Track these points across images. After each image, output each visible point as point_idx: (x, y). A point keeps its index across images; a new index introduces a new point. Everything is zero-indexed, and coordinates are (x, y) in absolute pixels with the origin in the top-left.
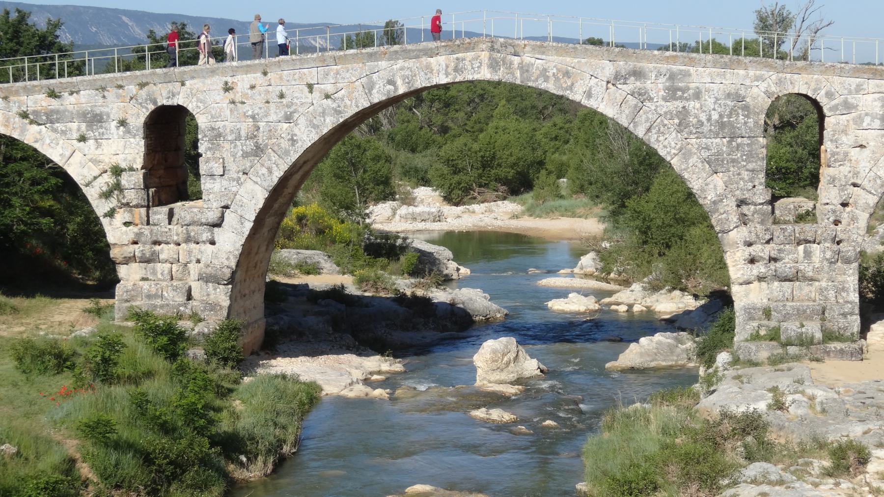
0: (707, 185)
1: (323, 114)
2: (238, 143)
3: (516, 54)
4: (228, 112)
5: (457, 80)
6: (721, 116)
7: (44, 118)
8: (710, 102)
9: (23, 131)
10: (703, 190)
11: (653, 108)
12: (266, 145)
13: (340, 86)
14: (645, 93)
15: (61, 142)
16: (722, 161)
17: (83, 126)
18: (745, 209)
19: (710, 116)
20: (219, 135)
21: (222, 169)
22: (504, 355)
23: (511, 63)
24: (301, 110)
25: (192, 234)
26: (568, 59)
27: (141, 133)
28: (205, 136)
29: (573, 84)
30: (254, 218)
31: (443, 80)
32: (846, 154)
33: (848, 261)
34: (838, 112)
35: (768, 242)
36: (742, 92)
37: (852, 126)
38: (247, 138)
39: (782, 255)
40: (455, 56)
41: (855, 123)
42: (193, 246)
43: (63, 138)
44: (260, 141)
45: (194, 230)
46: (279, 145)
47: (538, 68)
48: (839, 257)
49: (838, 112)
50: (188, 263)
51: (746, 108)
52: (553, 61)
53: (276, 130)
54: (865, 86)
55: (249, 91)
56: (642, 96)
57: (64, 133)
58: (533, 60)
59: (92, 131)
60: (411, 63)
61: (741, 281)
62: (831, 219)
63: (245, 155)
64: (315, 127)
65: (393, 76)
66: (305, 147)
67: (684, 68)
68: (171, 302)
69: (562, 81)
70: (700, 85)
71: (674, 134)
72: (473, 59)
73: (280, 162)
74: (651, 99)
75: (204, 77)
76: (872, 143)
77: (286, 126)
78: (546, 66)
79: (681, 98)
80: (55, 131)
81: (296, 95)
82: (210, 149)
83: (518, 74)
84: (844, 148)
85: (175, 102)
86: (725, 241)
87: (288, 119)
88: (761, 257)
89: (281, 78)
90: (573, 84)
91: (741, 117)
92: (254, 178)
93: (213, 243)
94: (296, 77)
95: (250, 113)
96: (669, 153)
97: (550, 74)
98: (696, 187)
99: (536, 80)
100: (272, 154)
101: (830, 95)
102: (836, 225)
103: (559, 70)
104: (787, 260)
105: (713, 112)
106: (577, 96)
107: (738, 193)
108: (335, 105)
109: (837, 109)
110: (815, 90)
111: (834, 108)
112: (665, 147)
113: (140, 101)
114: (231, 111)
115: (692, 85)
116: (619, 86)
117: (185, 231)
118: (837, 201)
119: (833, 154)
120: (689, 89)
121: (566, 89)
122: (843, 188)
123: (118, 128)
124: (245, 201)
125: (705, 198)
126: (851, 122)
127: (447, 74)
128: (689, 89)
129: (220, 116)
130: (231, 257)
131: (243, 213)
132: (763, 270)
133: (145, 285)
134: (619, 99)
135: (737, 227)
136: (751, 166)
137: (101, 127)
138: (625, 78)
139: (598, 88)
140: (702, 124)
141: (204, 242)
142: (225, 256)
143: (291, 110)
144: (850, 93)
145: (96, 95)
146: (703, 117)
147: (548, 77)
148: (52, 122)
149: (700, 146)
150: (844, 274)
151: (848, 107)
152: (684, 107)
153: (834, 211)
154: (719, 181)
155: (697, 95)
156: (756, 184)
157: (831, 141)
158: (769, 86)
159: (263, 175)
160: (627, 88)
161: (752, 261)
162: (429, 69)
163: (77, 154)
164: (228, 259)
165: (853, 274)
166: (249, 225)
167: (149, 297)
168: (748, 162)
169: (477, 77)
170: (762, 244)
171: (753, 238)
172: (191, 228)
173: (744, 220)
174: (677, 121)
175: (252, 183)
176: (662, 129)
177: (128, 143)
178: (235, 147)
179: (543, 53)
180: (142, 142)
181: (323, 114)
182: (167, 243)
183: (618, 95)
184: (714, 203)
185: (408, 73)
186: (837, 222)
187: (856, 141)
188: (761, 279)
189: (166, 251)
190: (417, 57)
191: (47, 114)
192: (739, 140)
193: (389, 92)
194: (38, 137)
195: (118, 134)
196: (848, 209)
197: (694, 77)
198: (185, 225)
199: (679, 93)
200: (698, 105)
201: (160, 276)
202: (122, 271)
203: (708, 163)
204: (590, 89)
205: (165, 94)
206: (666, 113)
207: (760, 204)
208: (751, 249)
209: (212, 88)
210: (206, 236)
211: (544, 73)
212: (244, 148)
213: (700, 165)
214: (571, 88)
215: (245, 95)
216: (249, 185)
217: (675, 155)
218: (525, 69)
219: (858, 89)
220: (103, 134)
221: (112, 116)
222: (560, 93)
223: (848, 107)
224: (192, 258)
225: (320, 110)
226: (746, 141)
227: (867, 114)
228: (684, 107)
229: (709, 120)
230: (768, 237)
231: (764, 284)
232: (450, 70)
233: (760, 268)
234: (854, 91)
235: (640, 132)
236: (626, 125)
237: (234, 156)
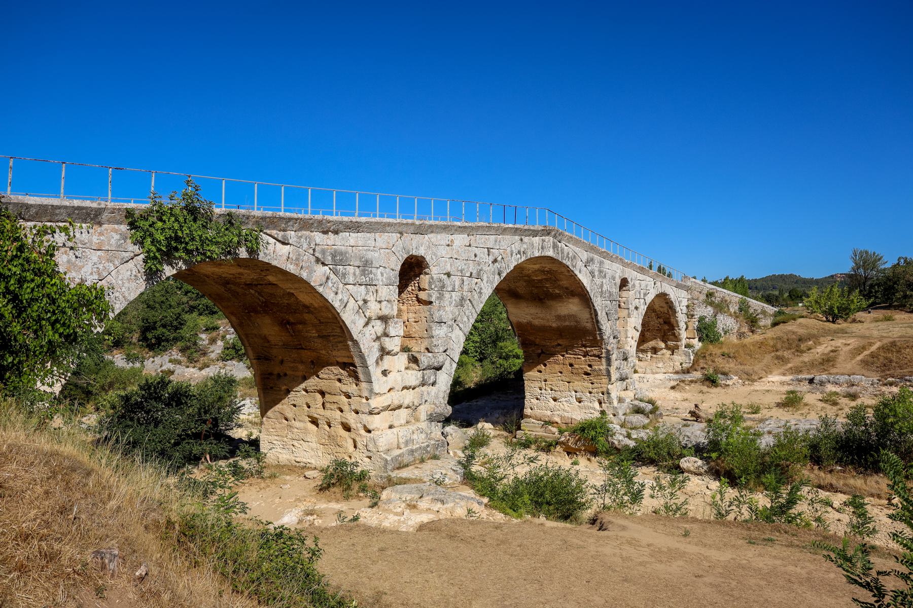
4: (449, 265)
9: (311, 271)
30: (457, 361)
43: (343, 281)
44: (464, 293)
51: (615, 284)
82: (438, 298)
92: (460, 325)
93: (433, 384)
97: (570, 256)
100: (470, 304)
106: (577, 272)
113: (399, 249)
123: (382, 274)
127: (539, 250)
142: (441, 395)
159: (465, 322)
164: (443, 398)
172: (425, 372)
191: (333, 256)
195: (382, 280)
214: (574, 267)
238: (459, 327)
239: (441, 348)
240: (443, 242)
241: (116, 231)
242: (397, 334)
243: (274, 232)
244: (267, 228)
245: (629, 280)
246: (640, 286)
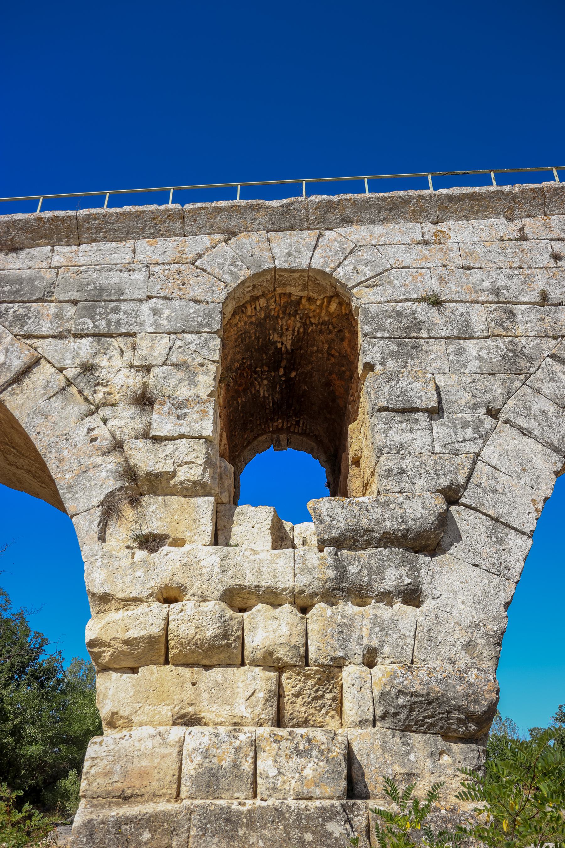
25: (353, 569)
28: (381, 328)
30: (530, 525)
59: (92, 318)
68: (291, 802)
92: (520, 421)
95: (486, 284)
117: (330, 561)
130: (481, 642)
137: (116, 310)
164: (469, 646)
177: (179, 343)
178: (459, 351)
212: (484, 354)
220: (118, 323)
238: (514, 425)
239: (420, 482)
240: (397, 238)
242: (185, 430)
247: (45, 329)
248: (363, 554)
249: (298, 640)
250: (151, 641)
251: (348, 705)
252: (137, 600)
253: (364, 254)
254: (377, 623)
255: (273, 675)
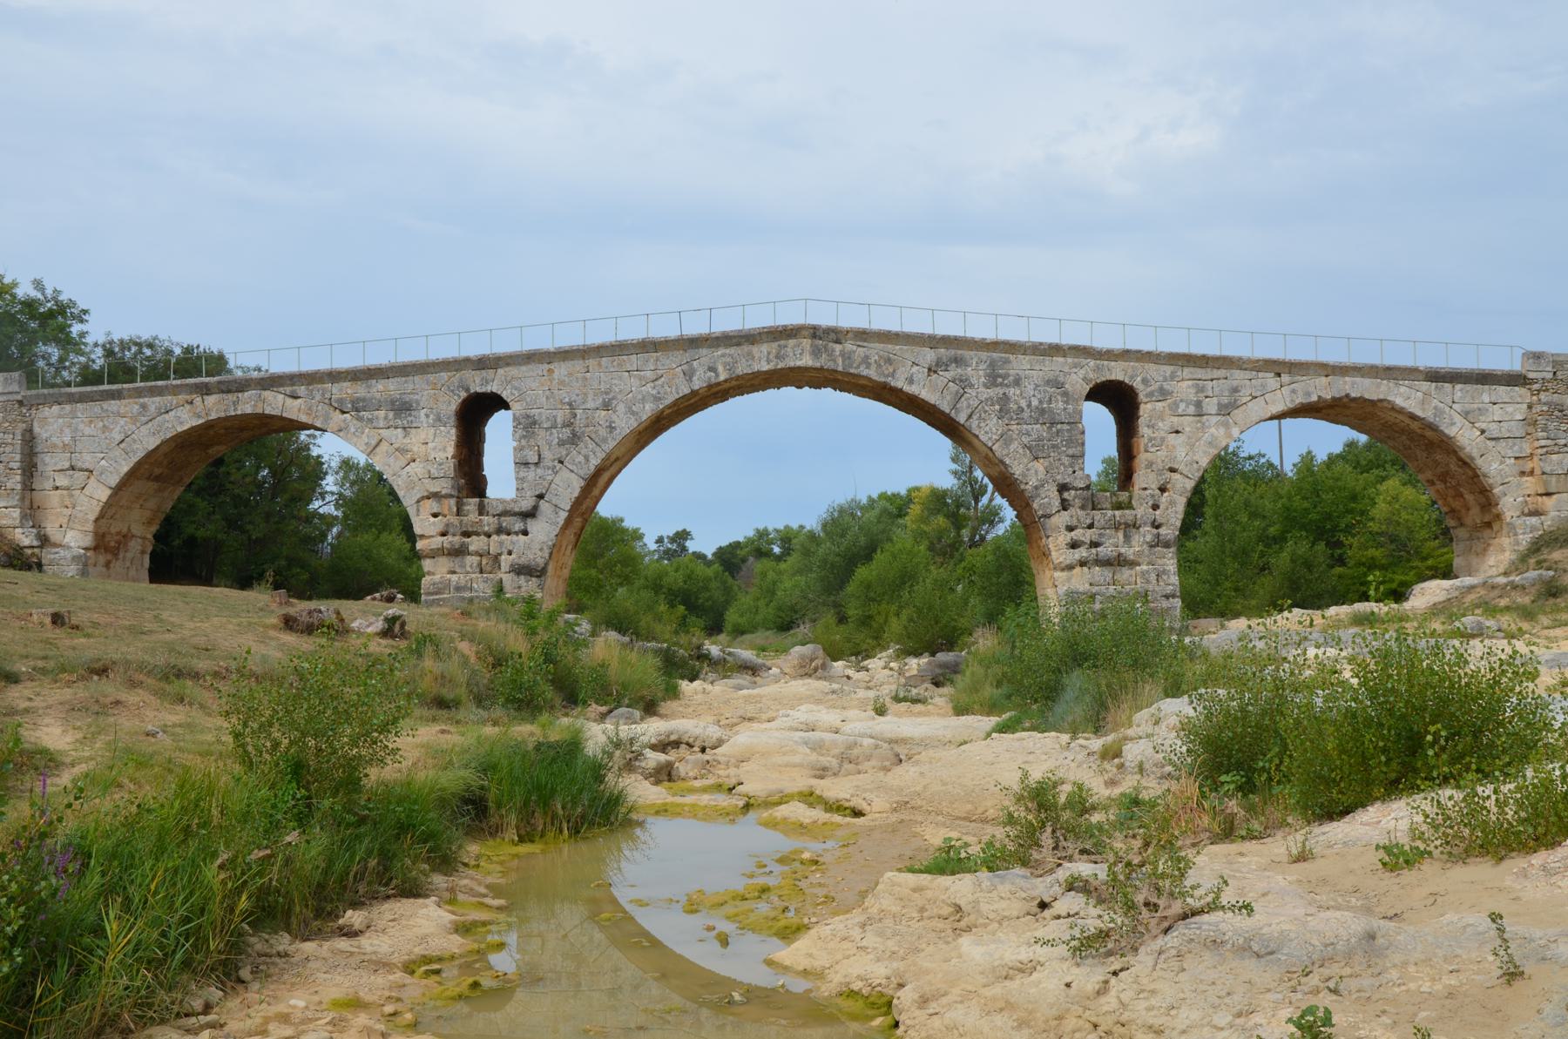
0: (1028, 470)
1: (643, 400)
2: (554, 431)
3: (838, 342)
4: (544, 399)
5: (779, 367)
6: (1041, 402)
7: (350, 406)
8: (1030, 389)
10: (1024, 475)
11: (974, 394)
12: (583, 433)
13: (660, 372)
14: (966, 380)
15: (367, 430)
16: (1043, 446)
17: (391, 415)
18: (1066, 495)
19: (1030, 402)
20: (535, 423)
21: (537, 457)
22: (812, 660)
23: (833, 351)
24: (619, 397)
25: (504, 524)
26: (890, 346)
27: (453, 421)
28: (520, 424)
29: (894, 371)
30: (568, 508)
31: (765, 367)
32: (1163, 439)
33: (1167, 545)
34: (1154, 399)
35: (1091, 526)
36: (1061, 379)
37: (1168, 411)
38: (565, 425)
39: (1103, 540)
40: (777, 344)
41: (1170, 409)
42: (504, 537)
44: (577, 429)
45: (506, 522)
46: (596, 432)
47: (859, 356)
48: (1158, 542)
49: (1154, 399)
50: (500, 554)
51: (1065, 394)
52: (875, 350)
53: (594, 418)
54: (1179, 373)
55: (566, 379)
56: (964, 383)
57: (370, 421)
58: (855, 348)
60: (732, 351)
61: (1063, 565)
62: (1150, 503)
63: (562, 443)
64: (633, 413)
65: (715, 362)
66: (624, 434)
67: (1003, 355)
69: (884, 368)
70: (1020, 373)
71: (995, 420)
72: (795, 346)
73: (598, 449)
74: (972, 386)
75: (520, 364)
76: (1187, 429)
77: (603, 413)
78: (868, 353)
79: (1001, 384)
80: (360, 419)
81: (616, 382)
82: (524, 437)
83: (840, 361)
84: (1163, 434)
85: (488, 389)
86: (1048, 526)
87: (607, 406)
88: (1083, 542)
89: (600, 365)
90: (894, 371)
91: (1061, 403)
93: (525, 533)
94: (615, 363)
95: (567, 400)
96: (990, 439)
98: (1017, 473)
99: (858, 367)
100: (590, 441)
101: (1145, 381)
102: (1154, 510)
103: (880, 357)
104: (1107, 545)
105: (1032, 399)
107: (1059, 477)
108: (654, 392)
109: (1153, 395)
110: (1131, 377)
111: (1151, 394)
112: (986, 433)
114: (547, 398)
115: (1011, 372)
116: (941, 373)
118: (1155, 486)
119: (1151, 439)
120: (1009, 375)
121: (888, 376)
122: (1160, 472)
123: (427, 416)
124: (560, 489)
125: (1027, 484)
126: (1167, 408)
127: (768, 361)
128: (1009, 375)
129: (536, 403)
131: (558, 502)
132: (1084, 554)
133: (454, 578)
134: (941, 387)
135: (1059, 511)
136: (1070, 452)
137: (410, 415)
138: (947, 365)
139: (920, 373)
140: (1023, 410)
141: (517, 533)
143: (610, 397)
144: (1165, 380)
145: (406, 382)
146: (1023, 404)
147: (870, 364)
148: (357, 410)
149: (1020, 432)
150: (1164, 557)
151: (1164, 394)
152: (1004, 394)
153: (1153, 496)
154: (1039, 466)
155: (1017, 382)
156: (1076, 469)
157: (1148, 426)
158: (1087, 372)
159: (580, 463)
160: (949, 375)
161: (1074, 545)
162: (750, 356)
163: (384, 442)
164: (541, 550)
165: (1172, 558)
166: (564, 515)
167: (458, 589)
168: (1068, 446)
169: (799, 363)
170: (1083, 528)
171: (1075, 522)
172: (503, 518)
173: (1065, 505)
174: (997, 407)
175: (568, 471)
176: (983, 415)
178: (551, 434)
179: (865, 341)
180: (453, 431)
181: (643, 400)
182: (478, 534)
183: (939, 382)
184: (1036, 488)
185: (729, 360)
186: (1155, 507)
187: (1172, 427)
188: (1083, 564)
189: (475, 543)
190: (738, 344)
191: (353, 402)
192: (1059, 426)
193: (709, 378)
194: (343, 425)
196: (1166, 494)
197: (1014, 364)
198: (498, 515)
199: (1000, 380)
200: (1018, 392)
201: (469, 569)
202: (427, 564)
203: (1029, 448)
204: (912, 376)
205: (478, 381)
206: (987, 399)
207: (1081, 489)
208: (1073, 533)
209: (527, 374)
210: (518, 526)
211: (865, 360)
213: (1021, 451)
214: (893, 375)
215: (562, 383)
216: (565, 474)
217: (997, 441)
218: (846, 356)
219: (1172, 377)
221: (422, 404)
222: (882, 380)
223: (1164, 394)
224: (504, 549)
225: (640, 397)
226: (1066, 427)
227: (1181, 401)
228: (1004, 394)
229: (1029, 406)
230: (1089, 521)
231: (1085, 569)
232: (771, 357)
233: (1082, 553)
234: (1169, 379)
235: (962, 418)
236: (947, 411)
237: (550, 446)
240: (531, 373)
241: (136, 403)
243: (281, 389)
244: (272, 386)
245: (1137, 384)
246: (1201, 390)
247: (381, 426)
248: (508, 519)
249: (486, 548)
250: (438, 549)
251: (502, 568)
252: (432, 536)
253: (515, 383)
254: (513, 543)
255: (479, 558)
